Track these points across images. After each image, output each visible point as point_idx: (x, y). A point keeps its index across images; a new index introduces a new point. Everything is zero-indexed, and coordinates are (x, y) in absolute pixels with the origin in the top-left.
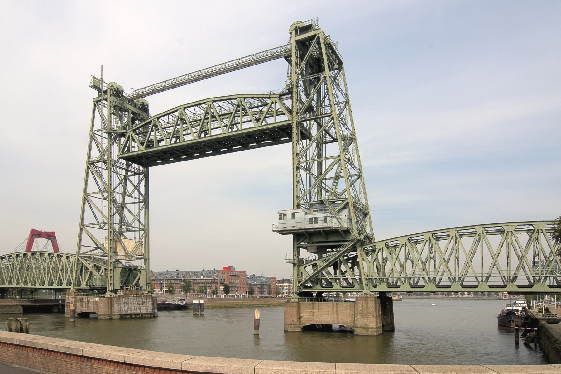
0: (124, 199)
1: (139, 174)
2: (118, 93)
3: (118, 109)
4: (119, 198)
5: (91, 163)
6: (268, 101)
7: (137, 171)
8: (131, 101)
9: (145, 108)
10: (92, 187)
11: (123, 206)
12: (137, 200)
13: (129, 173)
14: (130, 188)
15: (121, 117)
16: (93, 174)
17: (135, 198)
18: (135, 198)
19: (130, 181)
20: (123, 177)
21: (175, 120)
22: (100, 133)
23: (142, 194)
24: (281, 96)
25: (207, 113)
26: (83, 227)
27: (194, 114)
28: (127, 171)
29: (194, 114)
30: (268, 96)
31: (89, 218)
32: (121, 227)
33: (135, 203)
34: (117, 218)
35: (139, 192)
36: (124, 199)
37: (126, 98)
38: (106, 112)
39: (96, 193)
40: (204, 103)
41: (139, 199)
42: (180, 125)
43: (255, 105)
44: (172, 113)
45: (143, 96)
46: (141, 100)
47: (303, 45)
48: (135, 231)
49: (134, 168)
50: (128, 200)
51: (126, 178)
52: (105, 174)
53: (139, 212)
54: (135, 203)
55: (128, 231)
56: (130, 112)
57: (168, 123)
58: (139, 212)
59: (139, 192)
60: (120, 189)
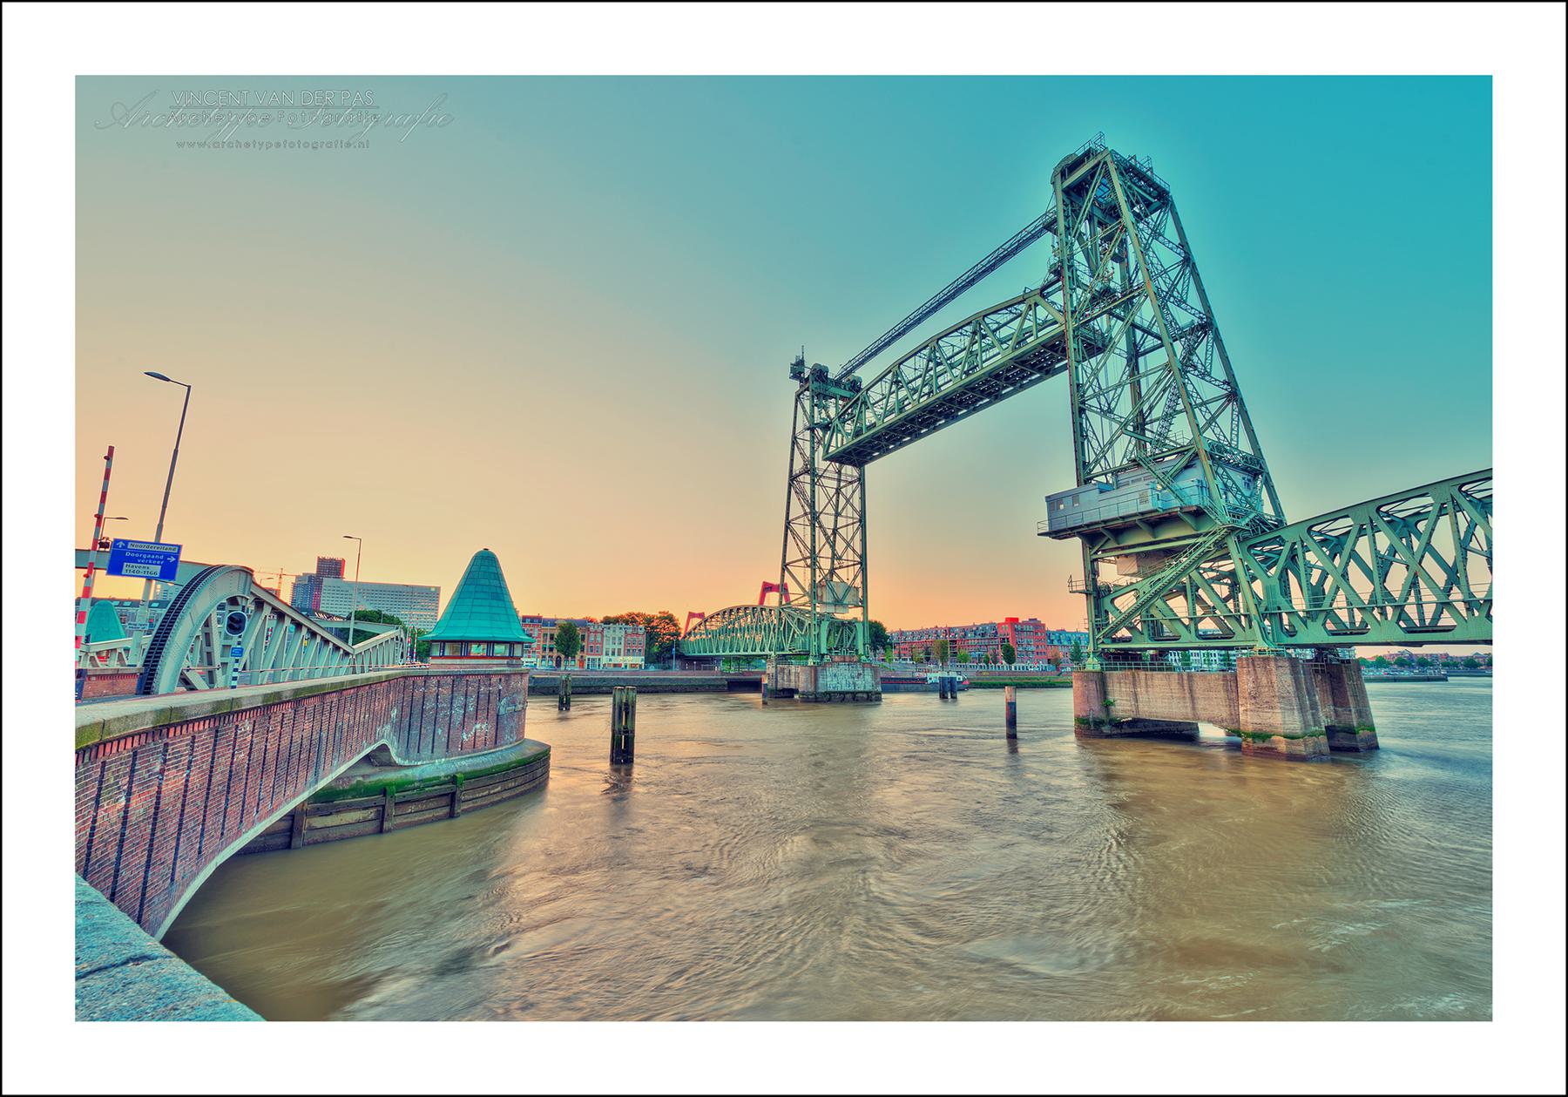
0: (836, 521)
1: (851, 483)
2: (820, 374)
3: (821, 396)
4: (827, 521)
5: (793, 478)
6: (1023, 307)
7: (850, 479)
8: (837, 383)
9: (855, 386)
10: (797, 509)
11: (835, 531)
12: (850, 521)
13: (842, 484)
14: (842, 501)
15: (825, 408)
16: (796, 492)
17: (847, 517)
18: (847, 517)
19: (843, 494)
20: (832, 492)
21: (888, 385)
22: (801, 436)
23: (856, 511)
24: (1043, 292)
25: (930, 360)
26: (785, 566)
27: (915, 369)
28: (839, 480)
29: (915, 369)
30: (1021, 299)
31: (793, 554)
32: (833, 562)
33: (847, 525)
34: (827, 552)
35: (852, 505)
36: (836, 521)
37: (832, 381)
38: (807, 404)
39: (798, 518)
40: (925, 348)
41: (853, 518)
42: (894, 392)
43: (1002, 322)
44: (884, 377)
45: (850, 372)
46: (850, 377)
47: (1075, 193)
48: (848, 566)
49: (846, 475)
50: (841, 521)
51: (838, 491)
52: (808, 488)
53: (852, 538)
54: (847, 525)
55: (840, 567)
56: (838, 397)
57: (883, 395)
58: (852, 538)
59: (852, 505)
60: (830, 510)
